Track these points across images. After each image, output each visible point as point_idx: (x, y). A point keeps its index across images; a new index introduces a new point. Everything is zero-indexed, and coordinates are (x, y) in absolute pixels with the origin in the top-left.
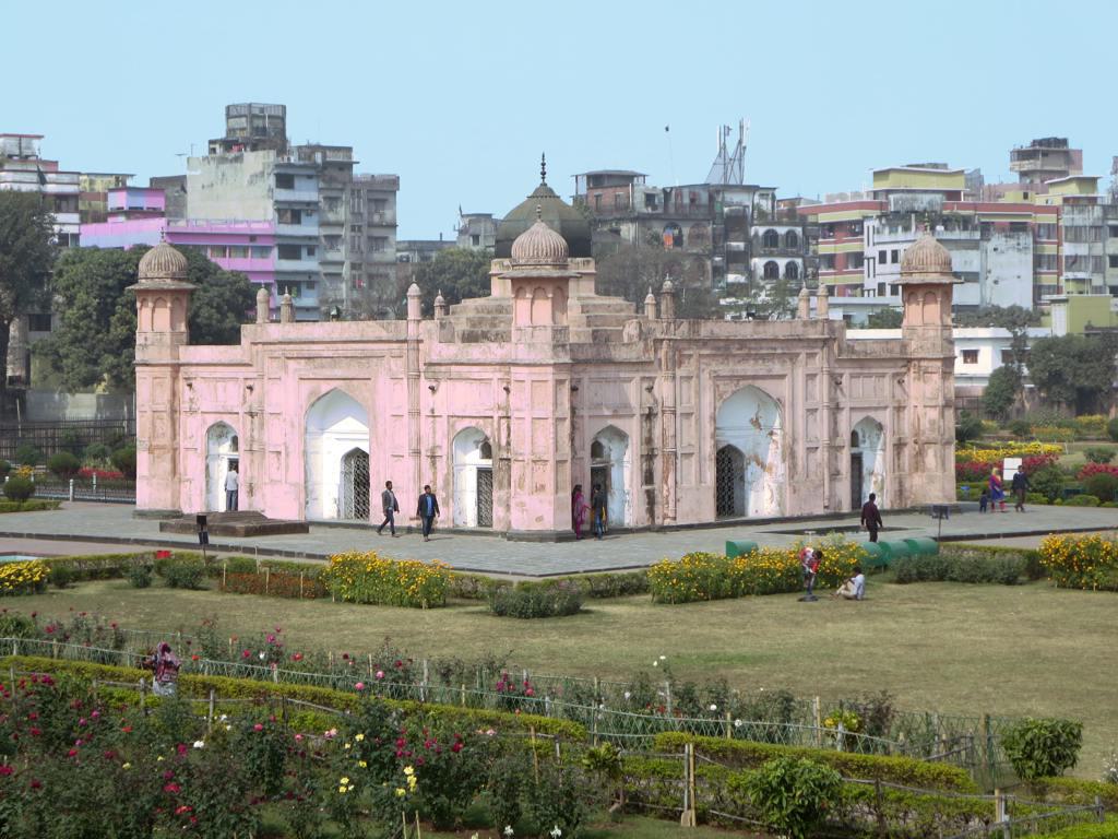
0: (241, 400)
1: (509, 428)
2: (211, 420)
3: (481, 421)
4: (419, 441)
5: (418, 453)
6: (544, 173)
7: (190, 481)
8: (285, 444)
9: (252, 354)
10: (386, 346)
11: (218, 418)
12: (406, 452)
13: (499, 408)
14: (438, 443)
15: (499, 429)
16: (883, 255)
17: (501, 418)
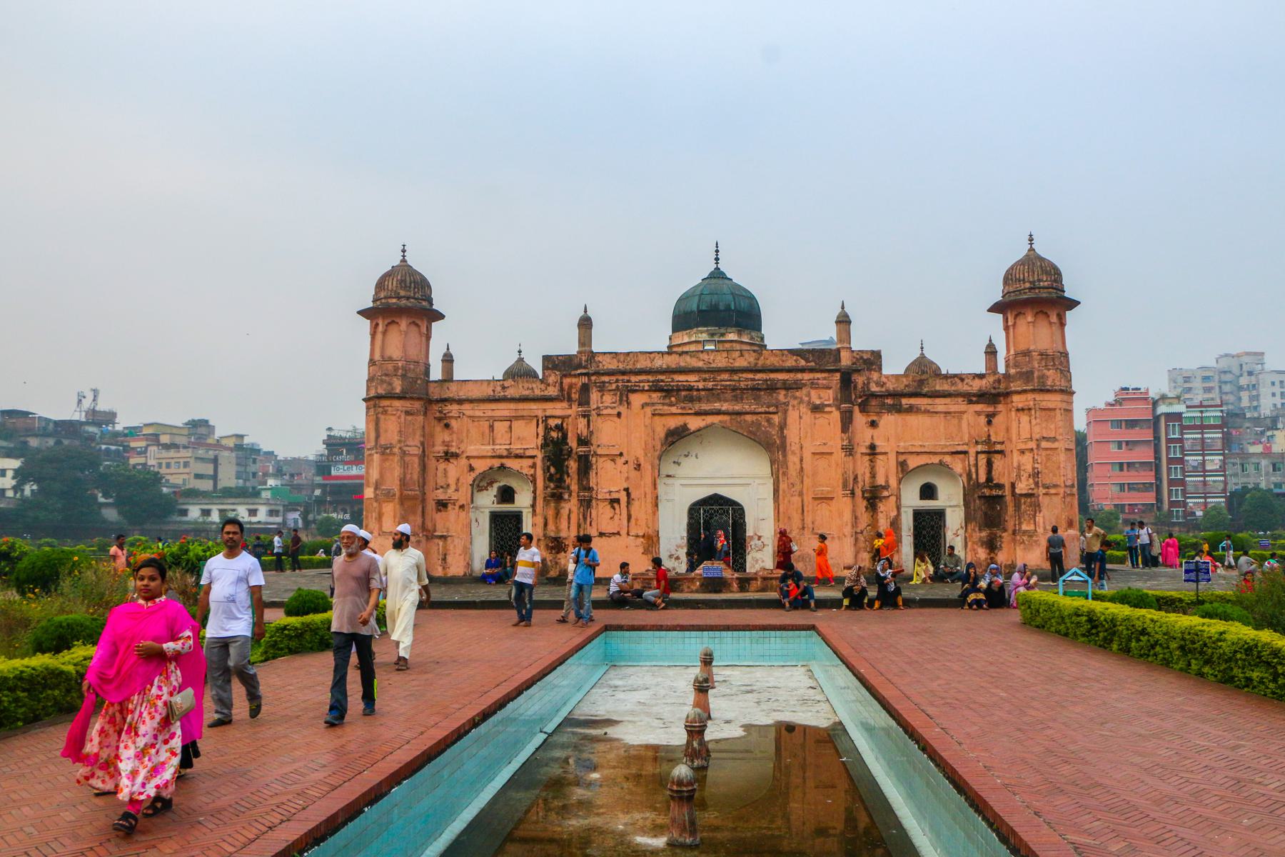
0: (540, 441)
1: (990, 464)
2: (481, 466)
3: (947, 459)
4: (856, 478)
5: (853, 493)
6: (717, 259)
7: (444, 538)
8: (627, 490)
9: (562, 389)
10: (807, 376)
11: (497, 463)
12: (840, 491)
13: (977, 443)
14: (880, 481)
15: (976, 465)
16: (160, 465)
17: (978, 453)
